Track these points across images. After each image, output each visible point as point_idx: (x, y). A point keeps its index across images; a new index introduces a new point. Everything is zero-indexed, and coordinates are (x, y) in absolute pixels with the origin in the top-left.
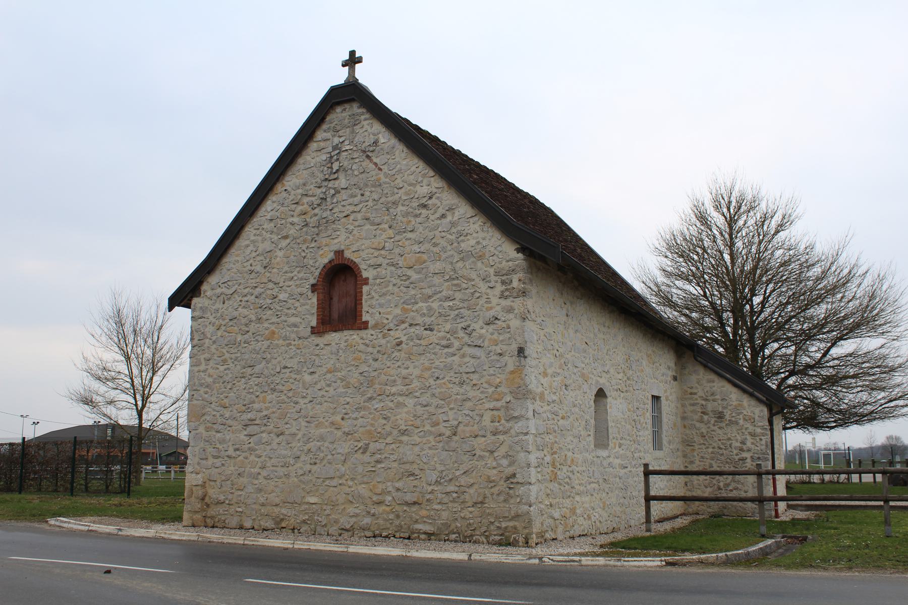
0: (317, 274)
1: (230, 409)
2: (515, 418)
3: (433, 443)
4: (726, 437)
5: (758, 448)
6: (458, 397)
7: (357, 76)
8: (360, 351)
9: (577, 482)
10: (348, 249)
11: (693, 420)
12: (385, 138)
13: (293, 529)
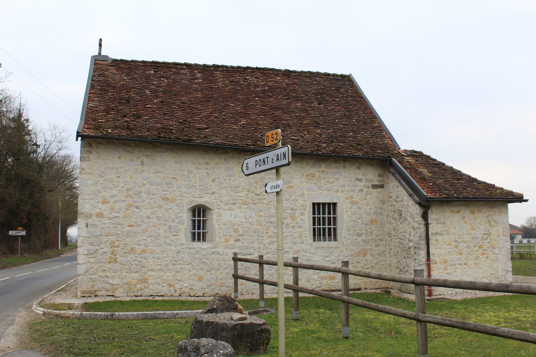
11: (390, 218)
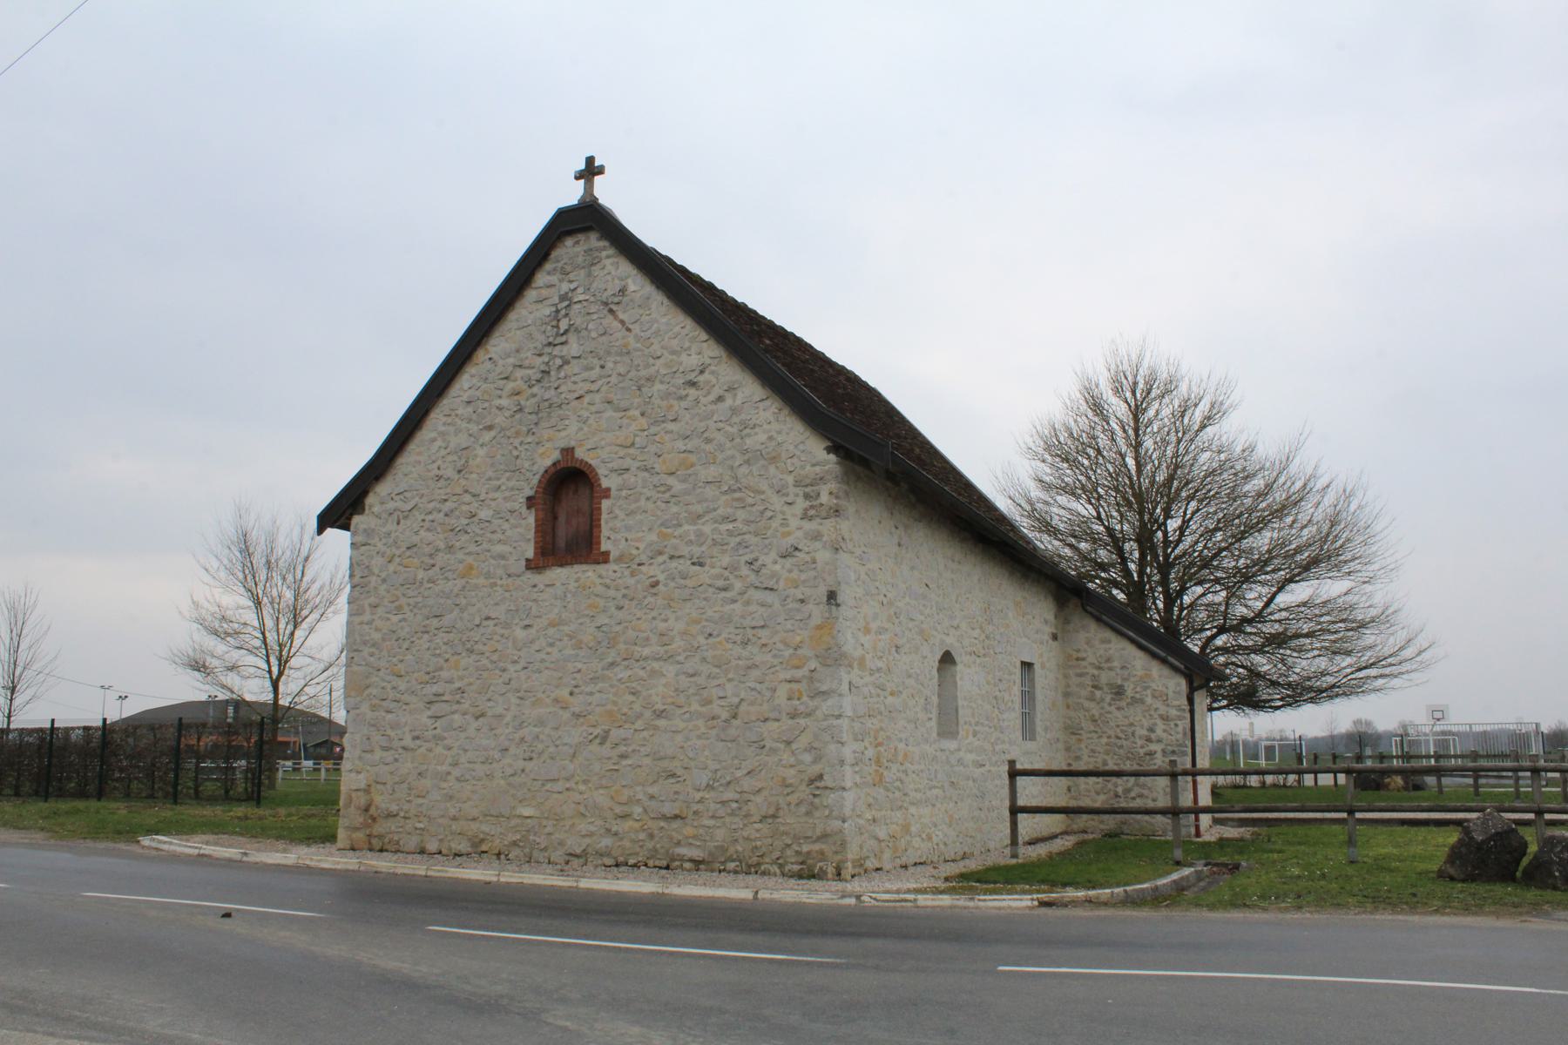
0: (535, 481)
1: (407, 678)
2: (823, 693)
3: (703, 729)
4: (1127, 722)
5: (1173, 738)
6: (740, 662)
7: (595, 194)
8: (597, 595)
9: (912, 786)
10: (581, 446)
11: (1080, 698)
12: (638, 284)
13: (499, 855)
